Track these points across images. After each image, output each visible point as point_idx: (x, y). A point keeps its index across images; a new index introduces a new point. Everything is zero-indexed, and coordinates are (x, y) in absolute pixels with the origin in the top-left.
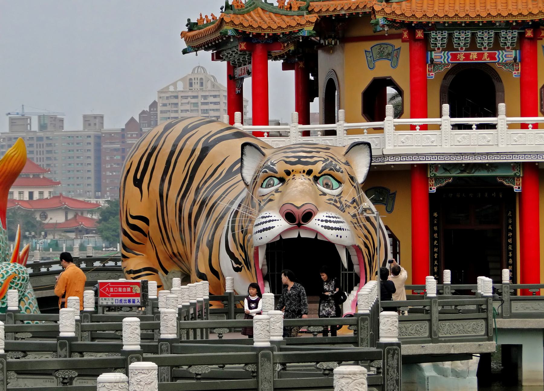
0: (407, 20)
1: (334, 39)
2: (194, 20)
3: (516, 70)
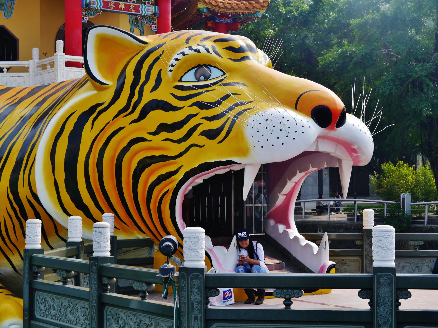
3: (154, 25)
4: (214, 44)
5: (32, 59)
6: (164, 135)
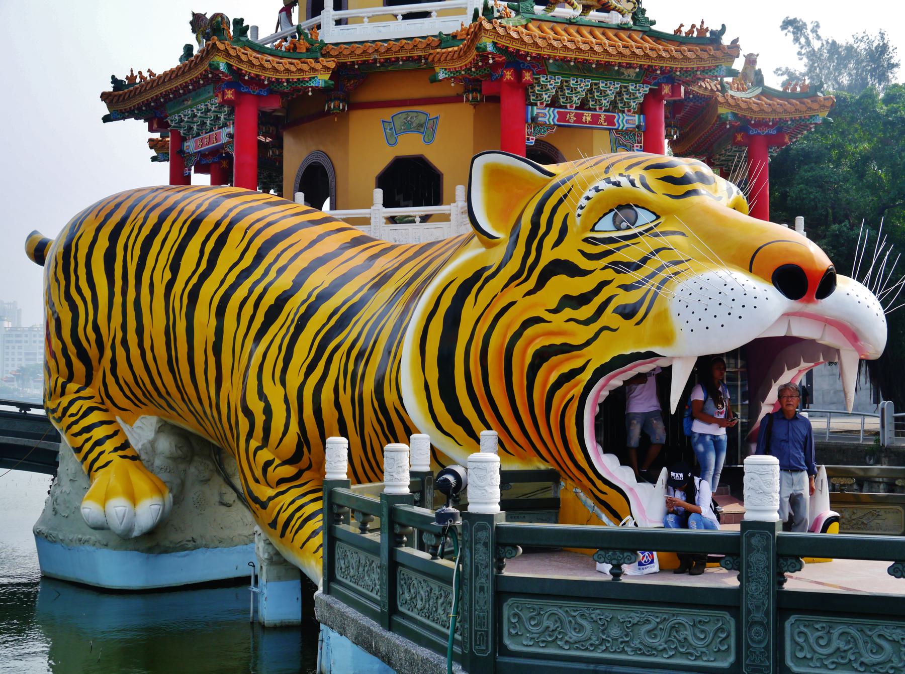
0: (523, 49)
1: (343, 101)
2: (121, 77)
4: (644, 173)
5: (454, 202)
6: (568, 312)
